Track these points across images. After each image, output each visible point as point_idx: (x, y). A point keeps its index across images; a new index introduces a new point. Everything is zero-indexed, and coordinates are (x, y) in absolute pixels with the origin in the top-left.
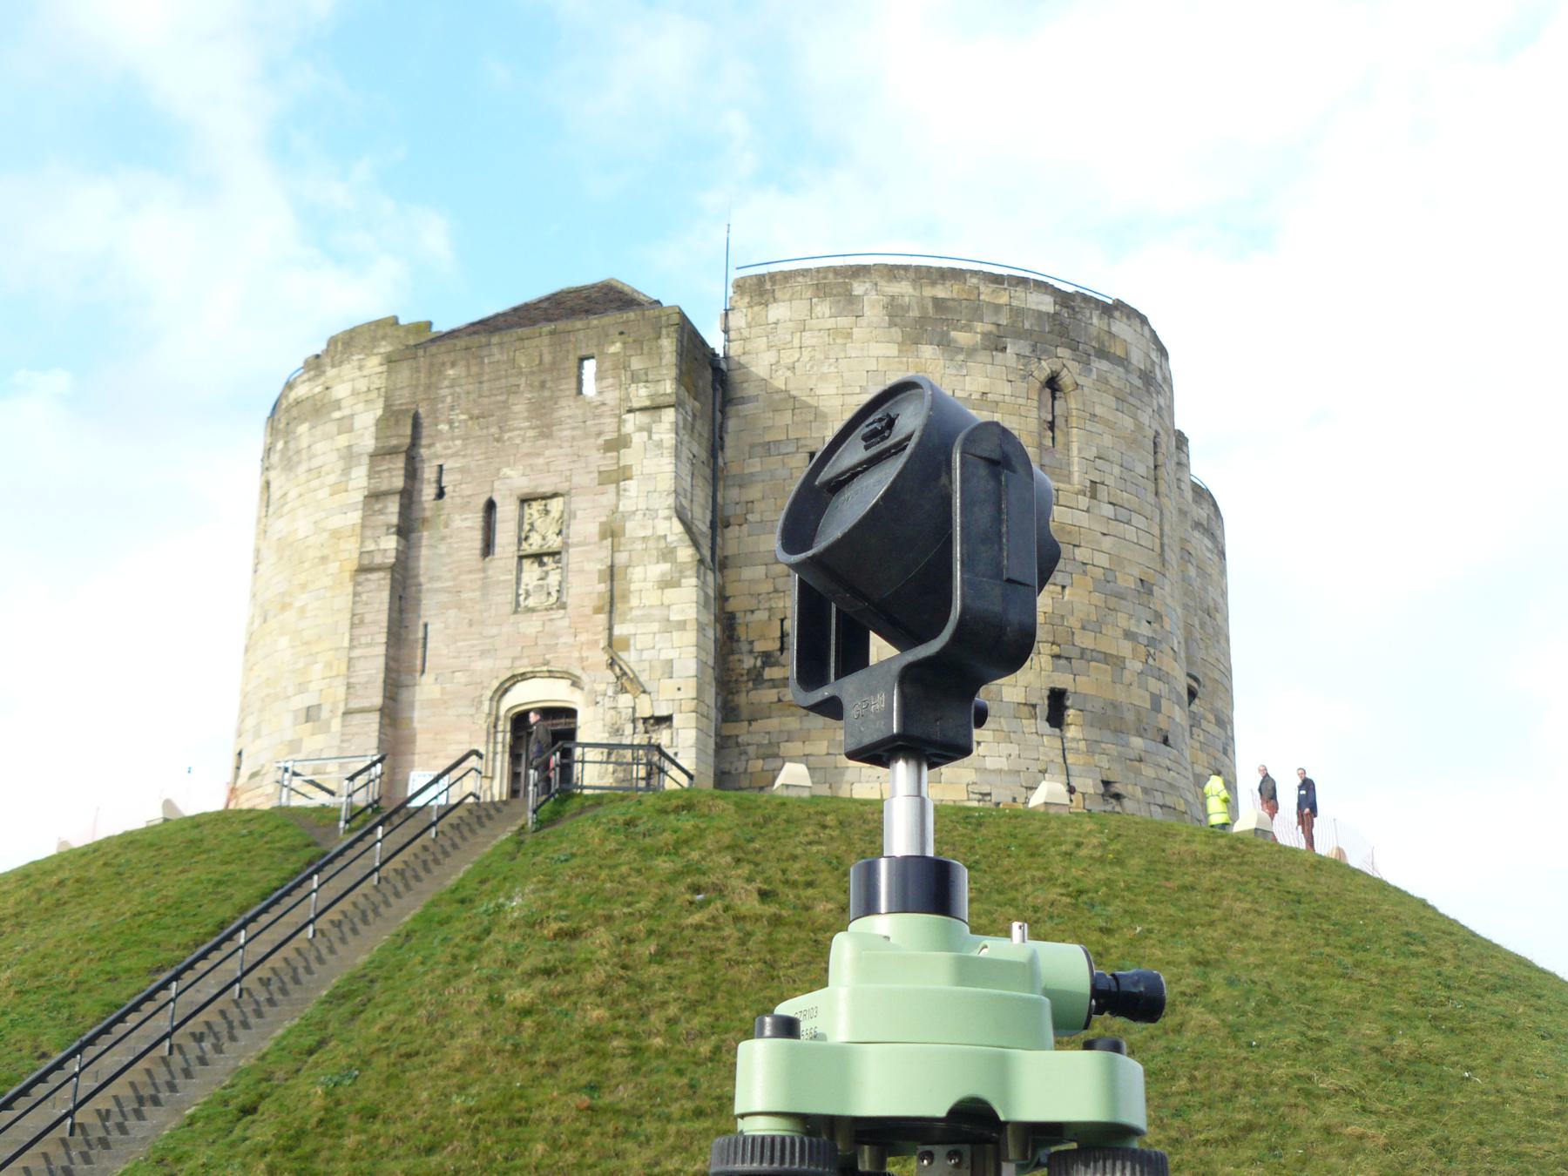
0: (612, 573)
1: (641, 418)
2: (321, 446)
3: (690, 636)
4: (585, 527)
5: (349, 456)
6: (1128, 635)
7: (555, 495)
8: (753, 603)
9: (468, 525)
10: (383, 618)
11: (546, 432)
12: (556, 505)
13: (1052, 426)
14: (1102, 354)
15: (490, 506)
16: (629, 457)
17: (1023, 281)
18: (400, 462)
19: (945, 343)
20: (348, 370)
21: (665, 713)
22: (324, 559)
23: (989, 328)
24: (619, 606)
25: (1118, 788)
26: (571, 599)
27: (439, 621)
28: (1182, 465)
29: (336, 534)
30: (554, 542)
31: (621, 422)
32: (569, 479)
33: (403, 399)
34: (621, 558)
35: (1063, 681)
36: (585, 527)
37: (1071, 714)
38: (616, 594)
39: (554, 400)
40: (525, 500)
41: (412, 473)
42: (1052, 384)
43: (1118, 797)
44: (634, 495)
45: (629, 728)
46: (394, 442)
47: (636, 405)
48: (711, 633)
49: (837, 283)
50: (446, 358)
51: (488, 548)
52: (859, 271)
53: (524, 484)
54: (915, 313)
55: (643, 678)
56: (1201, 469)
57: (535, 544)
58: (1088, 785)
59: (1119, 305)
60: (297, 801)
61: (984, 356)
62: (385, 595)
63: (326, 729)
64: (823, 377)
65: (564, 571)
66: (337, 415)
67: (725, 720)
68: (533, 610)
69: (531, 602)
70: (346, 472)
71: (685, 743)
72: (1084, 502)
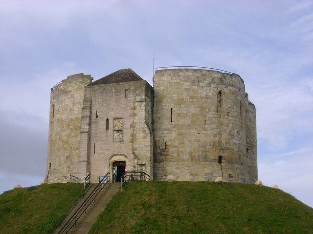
0: (133, 135)
1: (138, 103)
2: (67, 101)
3: (149, 148)
4: (127, 125)
5: (74, 103)
6: (234, 144)
7: (121, 118)
8: (160, 139)
9: (103, 123)
10: (87, 142)
12: (121, 120)
13: (220, 101)
14: (230, 85)
15: (108, 119)
16: (136, 111)
17: (214, 71)
18: (88, 110)
19: (199, 86)
20: (73, 84)
21: (144, 163)
23: (208, 82)
24: (135, 142)
25: (233, 175)
26: (125, 140)
27: (98, 145)
28: (247, 100)
29: (71, 120)
30: (121, 128)
31: (134, 104)
32: (124, 115)
33: (88, 96)
34: (135, 132)
35: (222, 154)
36: (127, 125)
37: (223, 161)
38: (134, 139)
39: (120, 98)
40: (115, 119)
41: (91, 113)
42: (220, 93)
43: (232, 177)
44: (137, 119)
45: (137, 166)
46: (87, 105)
47: (137, 100)
48: (152, 147)
49: (176, 71)
50: (99, 88)
51: (107, 128)
52: (181, 70)
54: (192, 79)
55: (139, 156)
56: (251, 99)
57: (117, 128)
58: (226, 175)
59: (234, 74)
60: (73, 181)
61: (206, 88)
62: (87, 138)
64: (174, 93)
66: (70, 94)
67: (154, 162)
68: (116, 142)
69: (116, 140)
70: (73, 106)
71: (148, 169)
72: (226, 117)
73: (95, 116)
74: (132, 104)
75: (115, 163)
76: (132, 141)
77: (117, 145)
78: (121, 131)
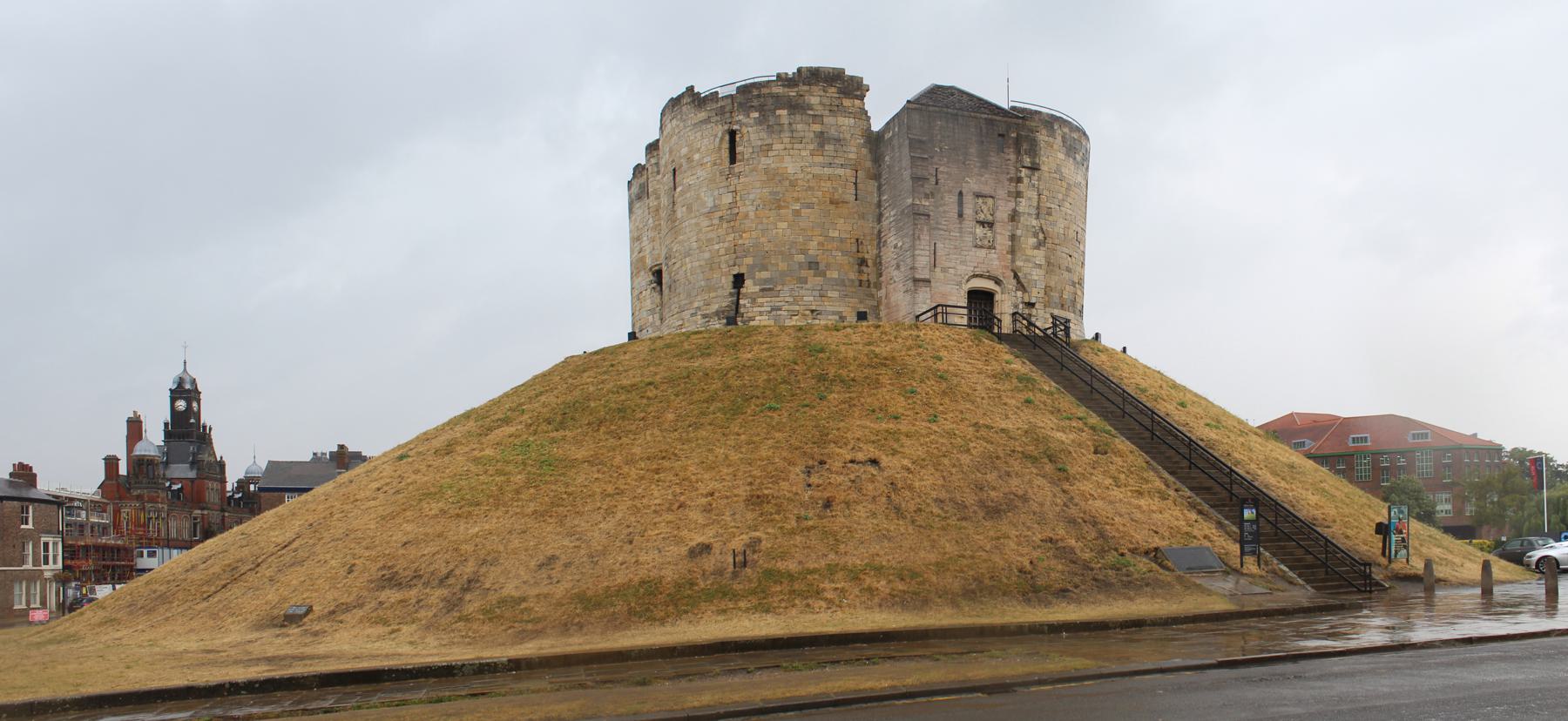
0: (1013, 238)
5: (822, 139)
9: (952, 199)
11: (985, 165)
12: (990, 201)
15: (961, 194)
16: (1022, 187)
22: (810, 188)
30: (990, 218)
34: (1019, 232)
36: (1003, 214)
40: (978, 196)
44: (1023, 206)
51: (961, 215)
53: (976, 188)
57: (982, 217)
63: (823, 274)
65: (995, 233)
70: (821, 145)
73: (933, 180)
74: (1012, 171)
75: (974, 295)
76: (1012, 251)
77: (984, 251)
78: (991, 225)
